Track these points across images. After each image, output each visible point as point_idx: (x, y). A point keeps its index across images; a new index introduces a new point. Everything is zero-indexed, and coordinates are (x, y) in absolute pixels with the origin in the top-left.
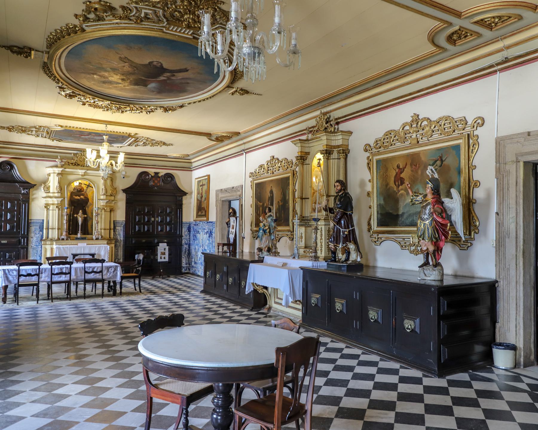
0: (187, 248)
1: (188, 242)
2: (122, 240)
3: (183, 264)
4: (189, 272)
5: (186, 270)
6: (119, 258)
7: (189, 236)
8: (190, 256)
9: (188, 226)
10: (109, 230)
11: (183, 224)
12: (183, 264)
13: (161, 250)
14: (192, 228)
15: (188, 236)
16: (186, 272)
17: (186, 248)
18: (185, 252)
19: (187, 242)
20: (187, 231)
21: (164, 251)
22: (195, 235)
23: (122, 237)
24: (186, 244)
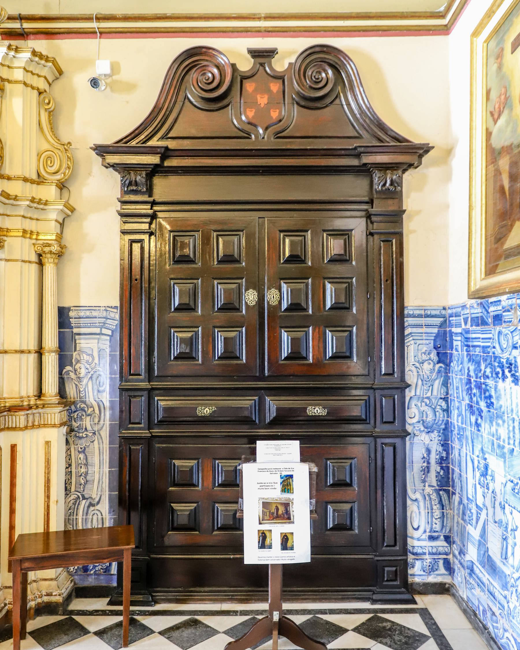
0: (436, 447)
1: (440, 415)
2: (107, 404)
3: (417, 534)
4: (447, 580)
5: (432, 569)
6: (95, 496)
7: (446, 384)
8: (450, 494)
9: (435, 330)
10: (32, 358)
11: (408, 321)
12: (417, 534)
13: (263, 486)
14: (457, 343)
15: (437, 384)
16: (432, 579)
17: (429, 451)
18: (426, 470)
19: (430, 418)
20: (434, 356)
21: (286, 496)
22: (479, 386)
23: (107, 387)
24: (429, 429)
